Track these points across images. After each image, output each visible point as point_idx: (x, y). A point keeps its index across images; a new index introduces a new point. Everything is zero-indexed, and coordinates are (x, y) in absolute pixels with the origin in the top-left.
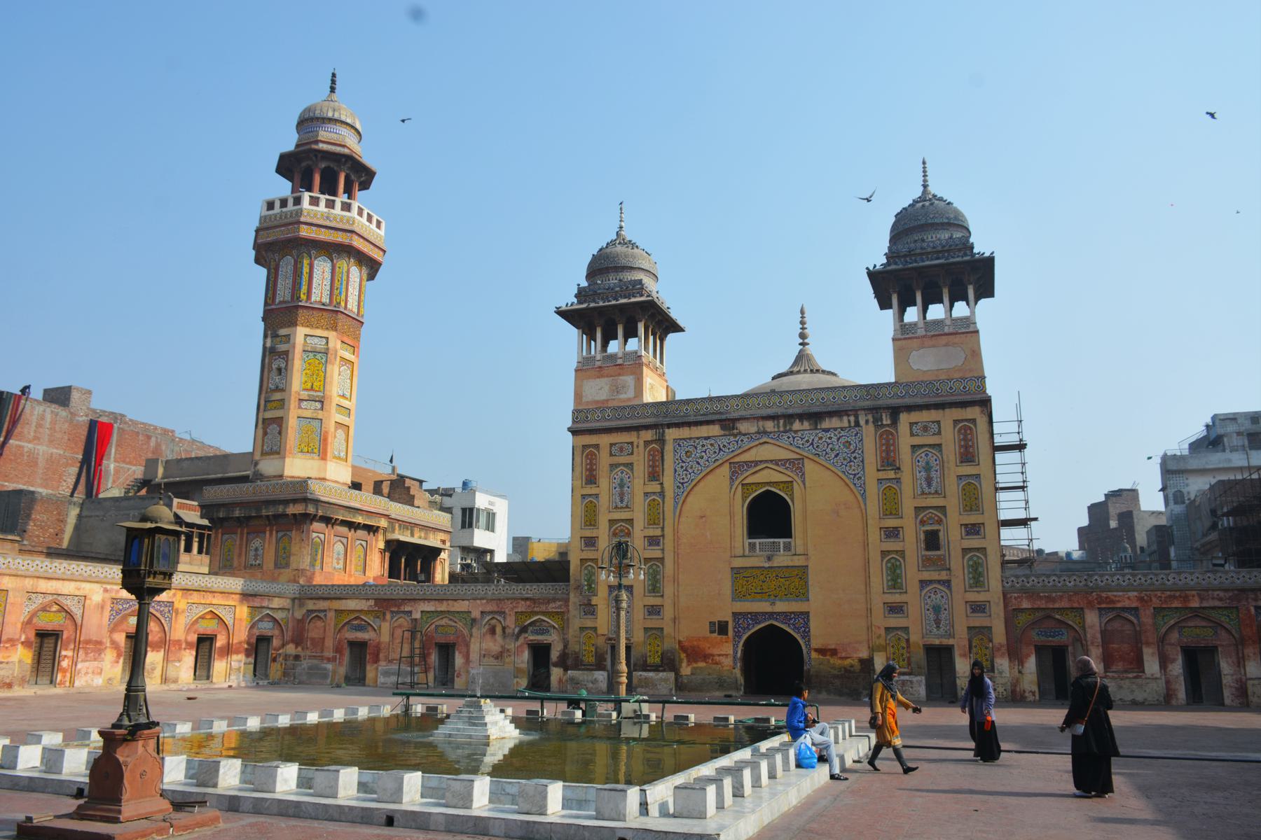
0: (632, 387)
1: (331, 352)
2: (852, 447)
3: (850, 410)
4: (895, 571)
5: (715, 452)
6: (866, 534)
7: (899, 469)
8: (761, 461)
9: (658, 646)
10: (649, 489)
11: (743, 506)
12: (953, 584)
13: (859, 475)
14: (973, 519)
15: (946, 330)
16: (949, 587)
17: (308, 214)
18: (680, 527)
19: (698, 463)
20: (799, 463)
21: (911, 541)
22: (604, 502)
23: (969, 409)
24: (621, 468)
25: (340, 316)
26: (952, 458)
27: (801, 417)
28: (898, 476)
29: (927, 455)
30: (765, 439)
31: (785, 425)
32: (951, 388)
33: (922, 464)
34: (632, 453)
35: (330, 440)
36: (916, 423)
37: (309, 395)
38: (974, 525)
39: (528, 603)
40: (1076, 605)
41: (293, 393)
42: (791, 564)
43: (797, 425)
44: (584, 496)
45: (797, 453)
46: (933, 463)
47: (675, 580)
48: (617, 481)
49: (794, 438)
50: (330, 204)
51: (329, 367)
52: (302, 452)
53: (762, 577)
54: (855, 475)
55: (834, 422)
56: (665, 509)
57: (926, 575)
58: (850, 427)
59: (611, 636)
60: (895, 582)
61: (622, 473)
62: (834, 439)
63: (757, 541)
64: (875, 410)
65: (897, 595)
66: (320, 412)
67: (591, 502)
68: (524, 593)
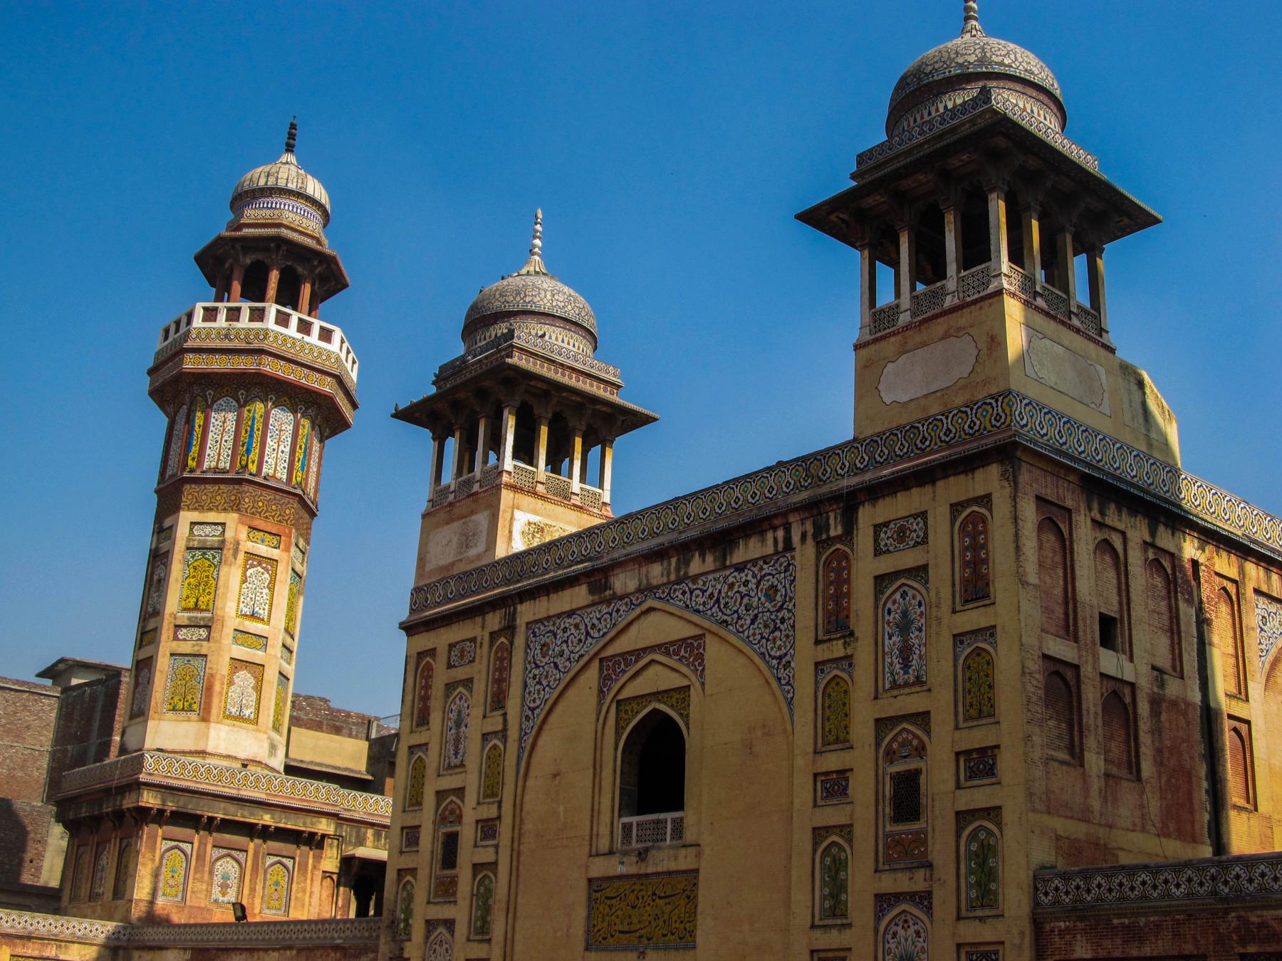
0: (485, 534)
1: (228, 545)
2: (778, 598)
3: (775, 516)
4: (837, 872)
5: (580, 640)
7: (852, 634)
8: (646, 650)
10: (489, 728)
11: (616, 749)
12: (936, 902)
13: (788, 658)
16: (929, 909)
17: (198, 335)
18: (527, 798)
20: (699, 646)
23: (979, 474)
25: (246, 487)
26: (946, 593)
28: (849, 651)
29: (904, 595)
30: (650, 603)
31: (678, 570)
33: (895, 616)
35: (217, 687)
36: (886, 524)
37: (189, 618)
38: (982, 751)
41: (166, 616)
42: (673, 866)
43: (696, 566)
45: (696, 625)
46: (915, 612)
49: (691, 593)
50: (234, 314)
51: (224, 569)
52: (174, 709)
54: (780, 658)
57: (888, 883)
58: (776, 553)
61: (461, 699)
63: (634, 819)
65: (835, 932)
66: (205, 643)
68: (336, 936)
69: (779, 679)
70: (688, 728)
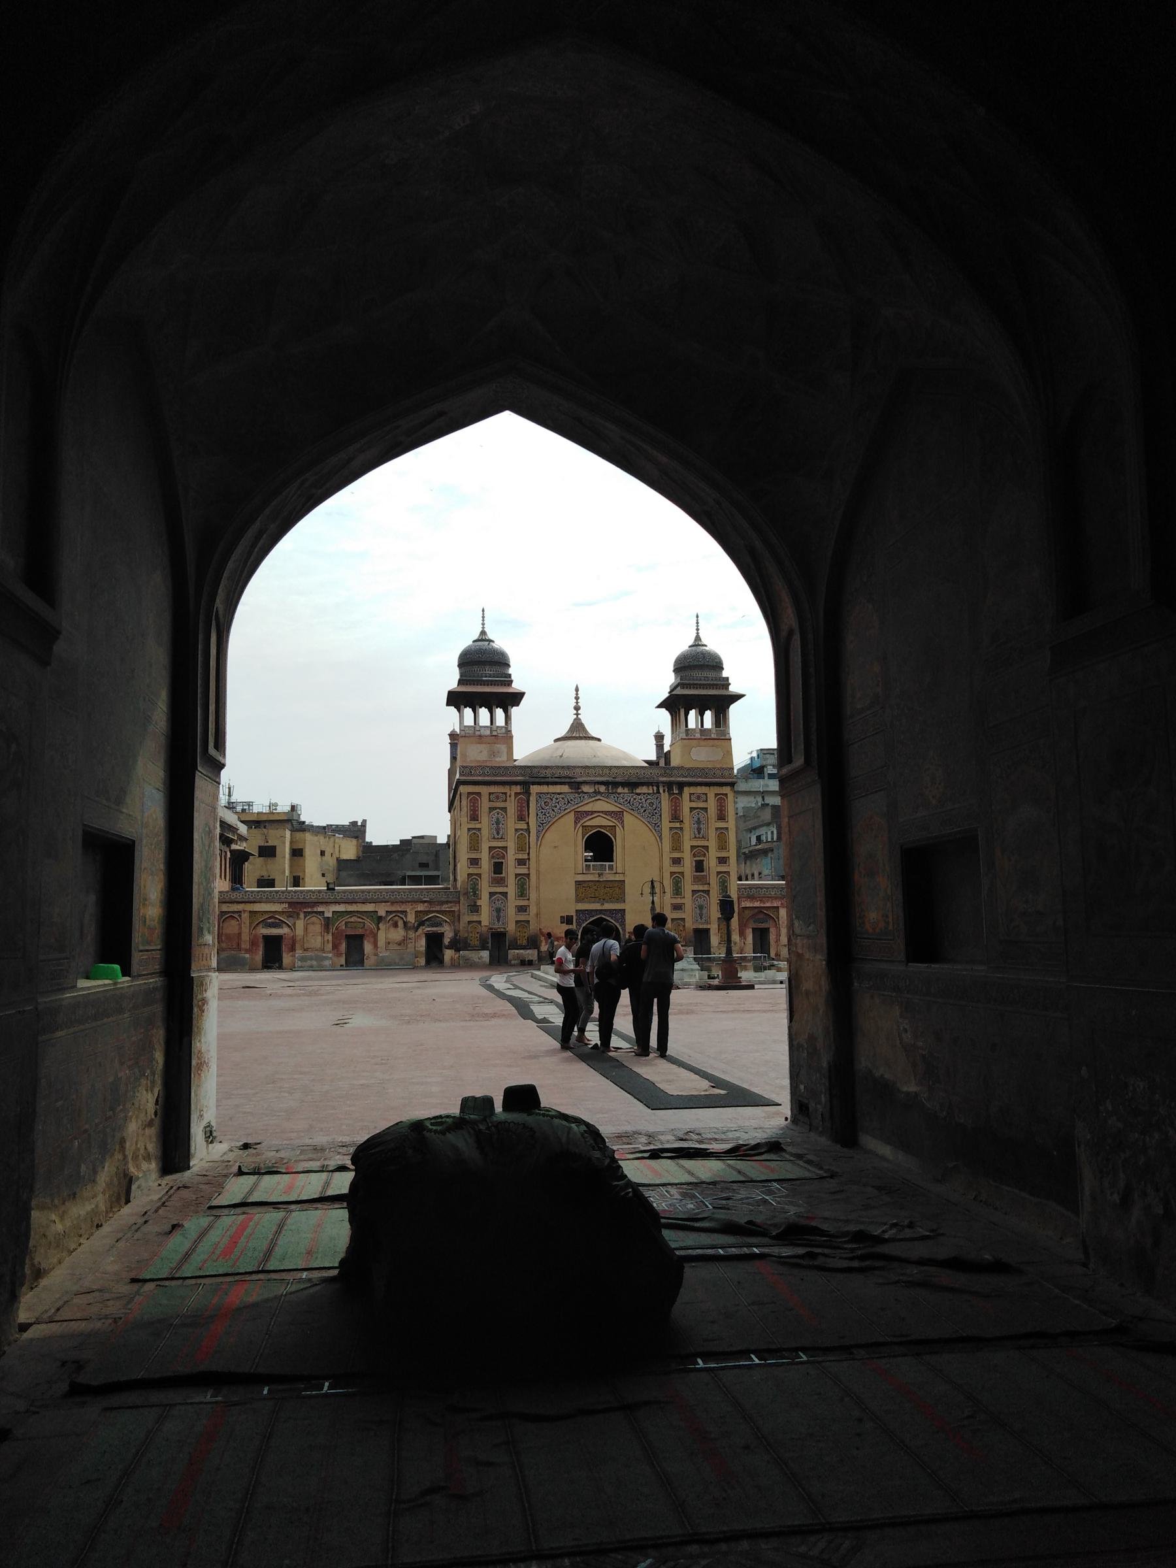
6: (661, 860)
7: (682, 821)
8: (595, 812)
9: (525, 932)
10: (519, 827)
14: (723, 854)
15: (713, 736)
16: (708, 894)
19: (553, 810)
20: (620, 814)
21: (688, 866)
22: (485, 833)
24: (498, 810)
26: (713, 816)
27: (624, 784)
28: (682, 826)
29: (698, 814)
31: (612, 789)
32: (714, 774)
33: (696, 819)
34: (506, 801)
36: (693, 794)
39: (426, 904)
40: (775, 905)
43: (620, 790)
44: (469, 830)
46: (702, 819)
47: (538, 888)
48: (494, 819)
49: (618, 798)
53: (595, 887)
54: (656, 824)
55: (644, 790)
56: (531, 840)
57: (696, 888)
59: (491, 926)
60: (677, 891)
61: (498, 814)
62: (644, 800)
64: (669, 786)
67: (475, 833)
69: (655, 830)
70: (615, 839)
